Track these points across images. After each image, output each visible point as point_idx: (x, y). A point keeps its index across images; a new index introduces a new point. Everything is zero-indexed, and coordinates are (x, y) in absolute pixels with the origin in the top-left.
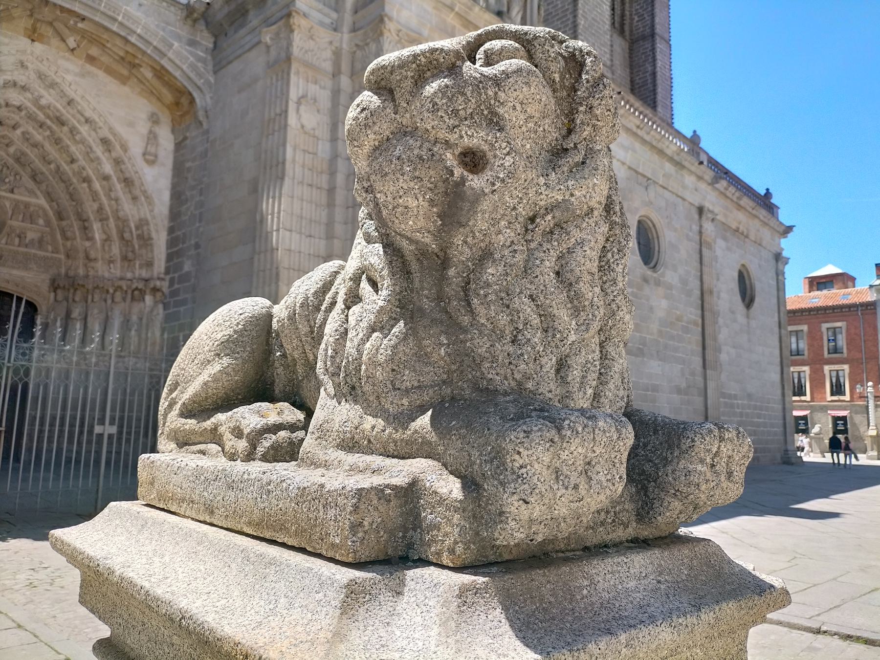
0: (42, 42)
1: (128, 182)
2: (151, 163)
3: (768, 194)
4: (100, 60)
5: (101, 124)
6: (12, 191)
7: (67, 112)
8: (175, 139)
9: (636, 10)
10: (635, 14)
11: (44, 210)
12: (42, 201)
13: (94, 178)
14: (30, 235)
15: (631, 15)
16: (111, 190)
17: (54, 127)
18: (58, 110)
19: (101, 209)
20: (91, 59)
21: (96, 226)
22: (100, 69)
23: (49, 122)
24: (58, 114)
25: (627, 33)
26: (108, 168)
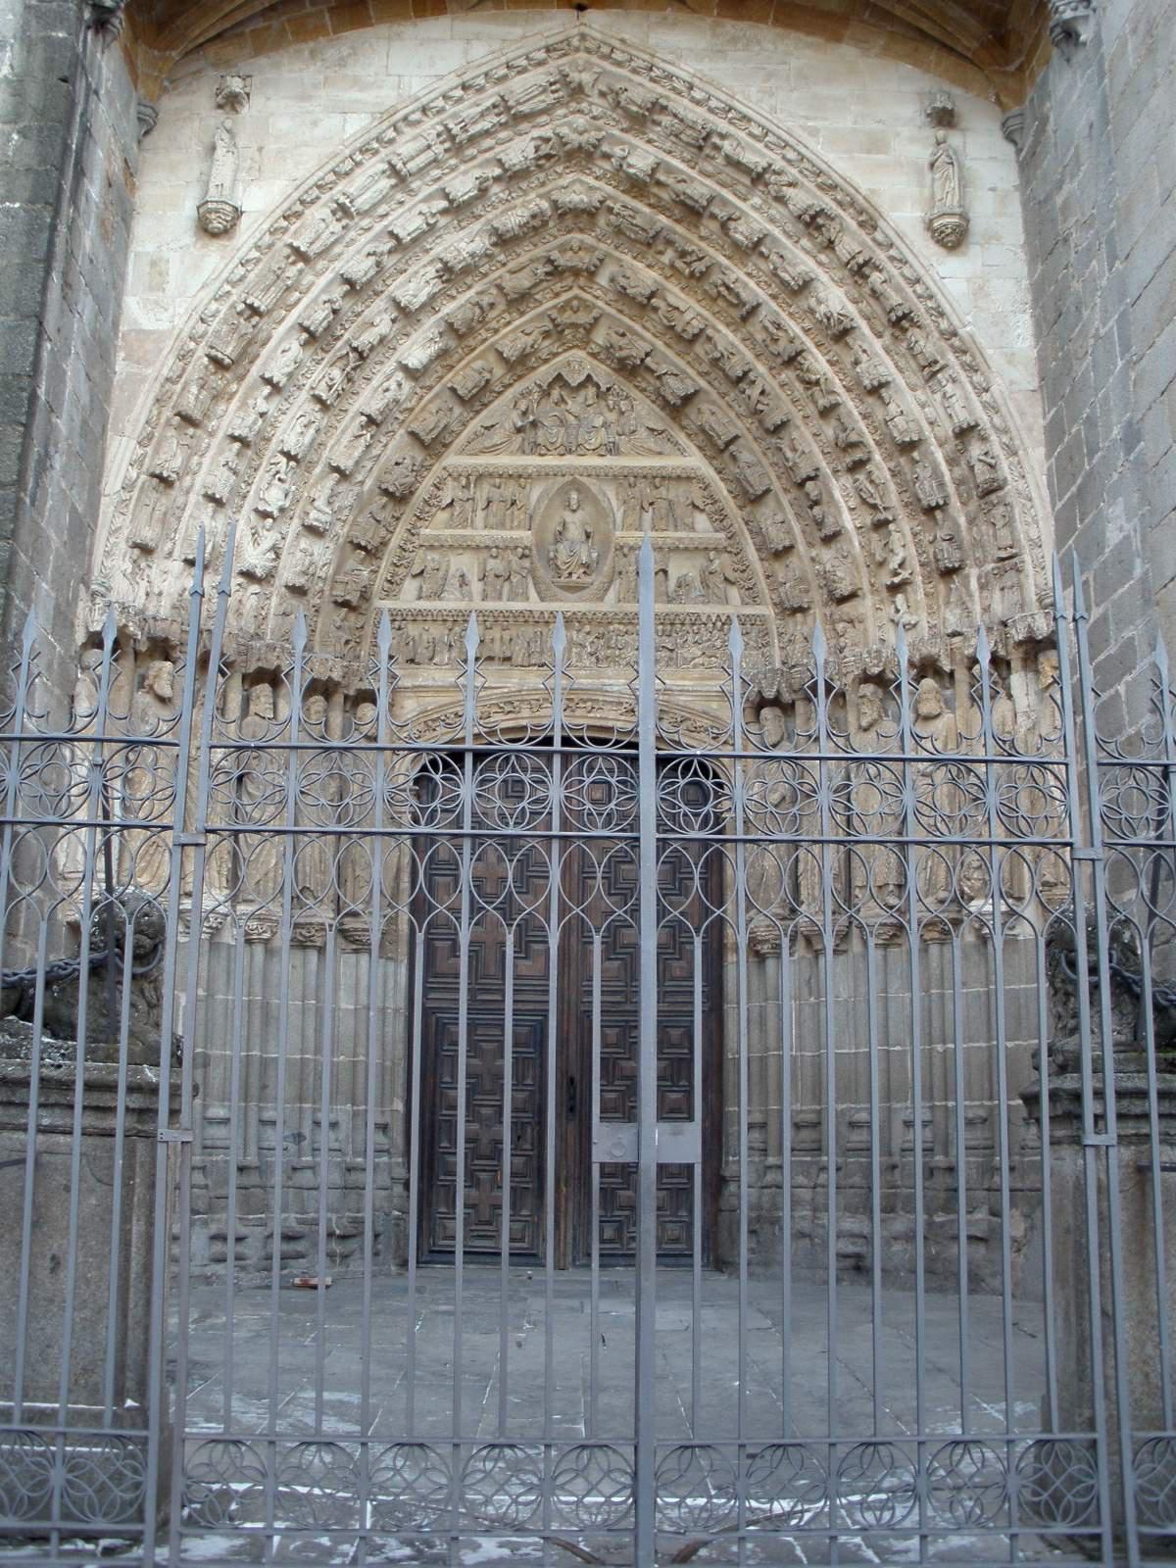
1: (900, 323)
2: (953, 237)
5: (793, 172)
6: (613, 449)
7: (701, 172)
12: (694, 460)
13: (809, 344)
17: (679, 228)
21: (840, 490)
23: (663, 220)
26: (834, 297)
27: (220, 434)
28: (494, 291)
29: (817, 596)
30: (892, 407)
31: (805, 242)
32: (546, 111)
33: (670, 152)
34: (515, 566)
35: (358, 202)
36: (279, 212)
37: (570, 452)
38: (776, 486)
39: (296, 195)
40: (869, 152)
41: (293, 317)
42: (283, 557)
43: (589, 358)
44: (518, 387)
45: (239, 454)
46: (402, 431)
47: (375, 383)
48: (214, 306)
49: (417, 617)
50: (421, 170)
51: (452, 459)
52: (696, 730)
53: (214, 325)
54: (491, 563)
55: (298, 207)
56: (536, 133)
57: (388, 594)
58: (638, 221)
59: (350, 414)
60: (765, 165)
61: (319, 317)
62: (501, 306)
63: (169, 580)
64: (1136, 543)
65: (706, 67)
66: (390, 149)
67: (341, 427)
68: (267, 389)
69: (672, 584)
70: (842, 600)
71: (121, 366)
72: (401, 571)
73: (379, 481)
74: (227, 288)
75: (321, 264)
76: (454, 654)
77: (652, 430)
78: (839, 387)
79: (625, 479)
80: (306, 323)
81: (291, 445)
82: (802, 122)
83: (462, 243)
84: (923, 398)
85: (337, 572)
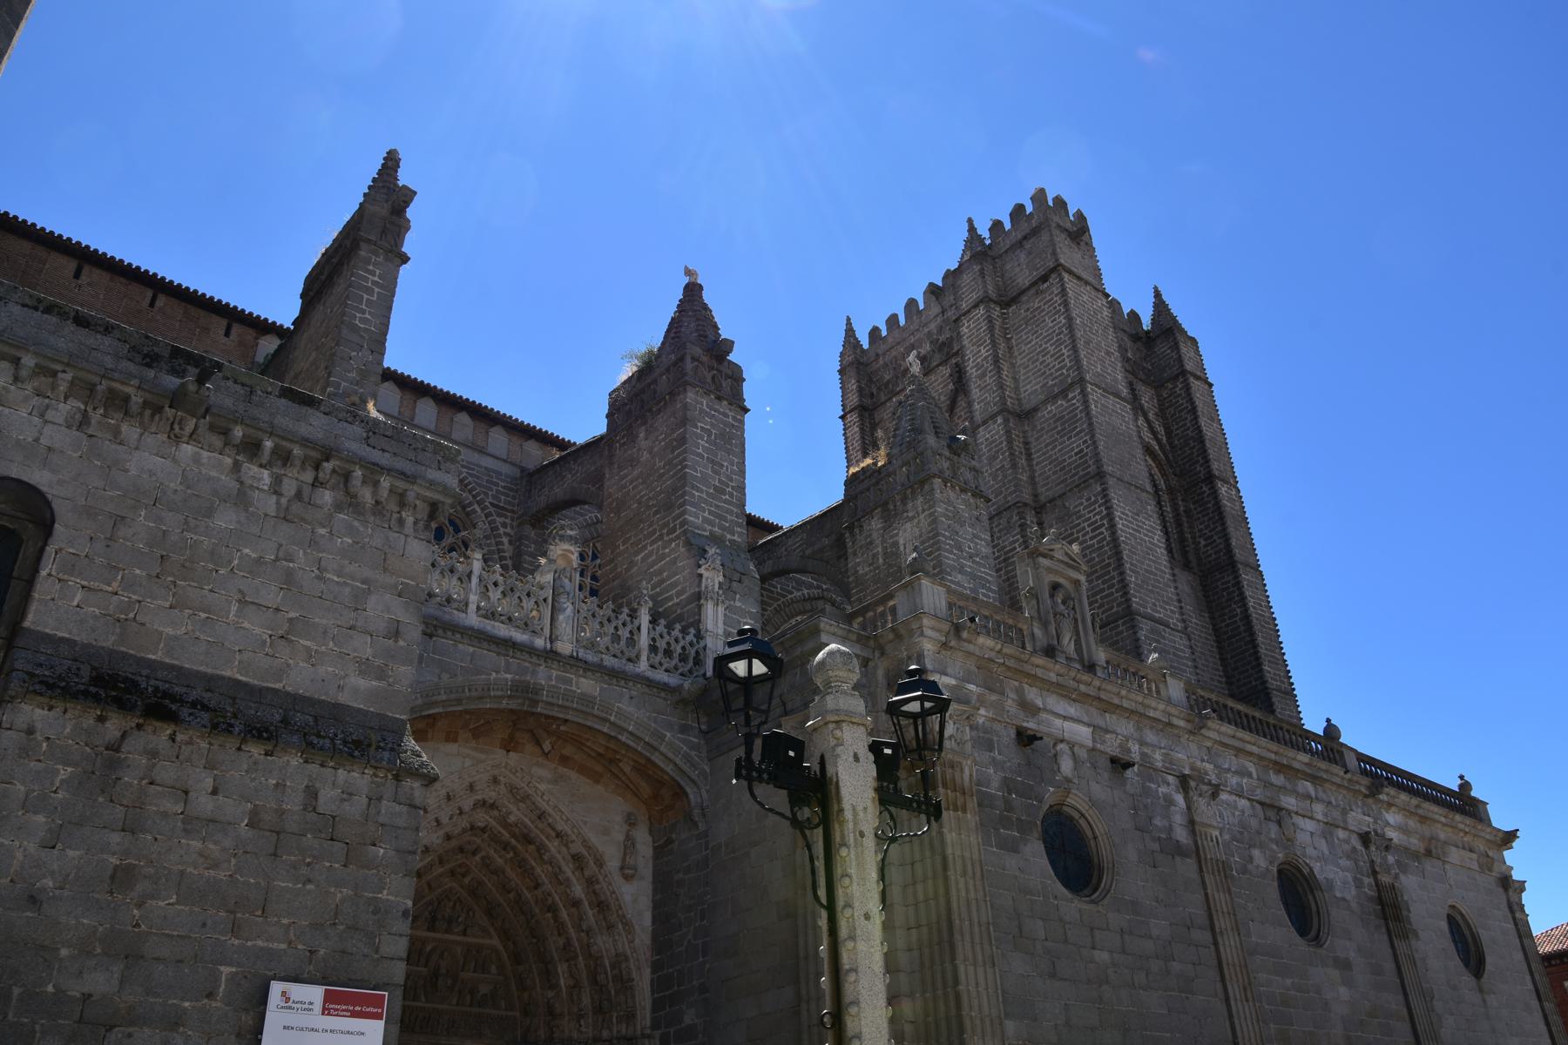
1: (601, 906)
2: (628, 878)
3: (1465, 786)
5: (574, 837)
6: (464, 933)
7: (536, 827)
8: (654, 842)
9: (1200, 531)
10: (1200, 537)
12: (495, 942)
15: (1194, 538)
16: (581, 919)
17: (519, 846)
19: (568, 944)
20: (564, 760)
21: (562, 968)
23: (513, 841)
24: (525, 831)
25: (1194, 563)
26: (578, 890)
65: (550, 787)
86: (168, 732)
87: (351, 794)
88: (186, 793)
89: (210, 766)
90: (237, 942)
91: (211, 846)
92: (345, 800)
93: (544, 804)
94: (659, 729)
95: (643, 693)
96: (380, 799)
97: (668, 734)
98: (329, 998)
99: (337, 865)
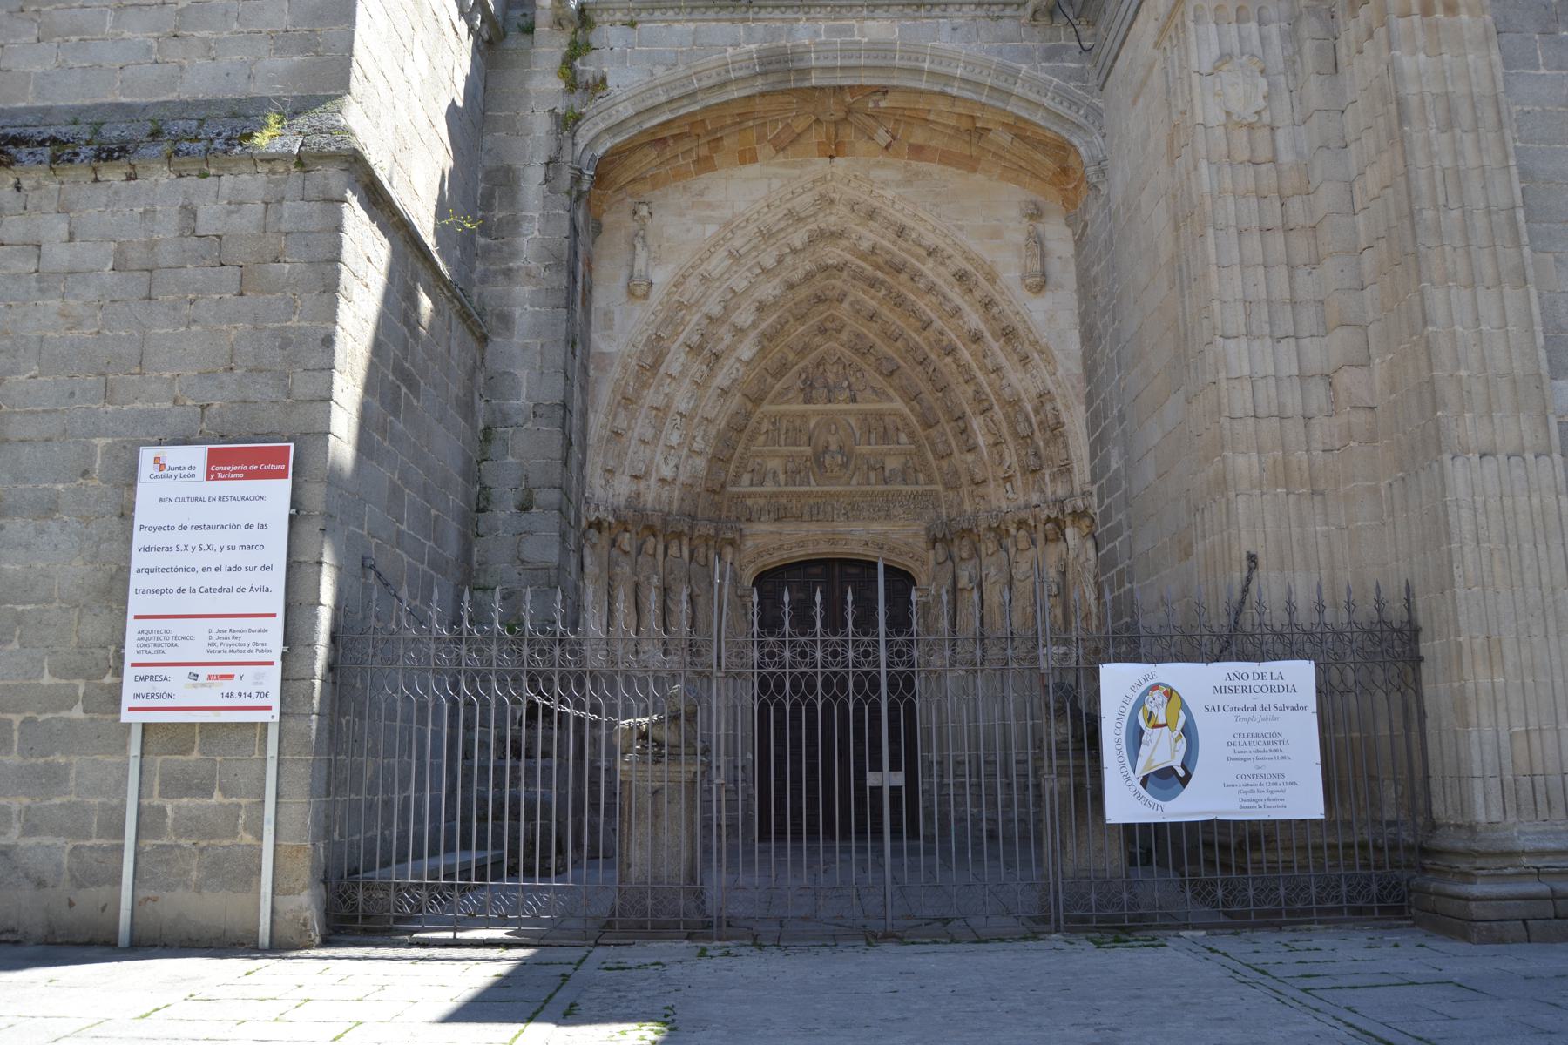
0: (844, 155)
1: (1008, 334)
2: (1040, 286)
4: (930, 147)
5: (950, 251)
6: (853, 400)
11: (903, 417)
12: (899, 404)
13: (960, 345)
14: (893, 463)
17: (888, 279)
18: (888, 252)
19: (978, 395)
20: (917, 151)
21: (977, 423)
22: (932, 161)
23: (879, 274)
24: (888, 257)
26: (974, 319)
27: (646, 406)
28: (787, 314)
29: (965, 479)
30: (1004, 381)
31: (957, 289)
32: (815, 214)
33: (882, 237)
34: (802, 467)
35: (713, 274)
36: (672, 283)
37: (830, 401)
38: (943, 420)
39: (680, 273)
40: (992, 239)
41: (681, 339)
42: (681, 468)
43: (839, 347)
44: (801, 365)
45: (656, 416)
46: (739, 395)
47: (724, 370)
48: (639, 338)
49: (750, 495)
50: (748, 252)
51: (766, 407)
52: (901, 554)
53: (640, 347)
54: (790, 465)
55: (682, 280)
56: (808, 227)
57: (734, 484)
58: (866, 273)
59: (712, 388)
60: (934, 247)
61: (696, 338)
62: (792, 321)
63: (622, 487)
64: (1123, 470)
65: (901, 190)
66: (730, 243)
67: (708, 395)
68: (669, 380)
69: (887, 473)
70: (977, 484)
71: (592, 373)
72: (741, 470)
73: (728, 424)
74: (646, 327)
75: (694, 309)
76: (772, 515)
77: (872, 387)
78: (974, 365)
79: (864, 416)
80: (689, 343)
81: (682, 408)
82: (955, 222)
83: (769, 290)
84: (1020, 377)
85: (707, 474)
86: (12, 181)
87: (241, 203)
88: (39, 246)
89: (64, 209)
90: (110, 408)
91: (72, 302)
92: (233, 212)
93: (899, 215)
94: (1008, 63)
95: (974, 18)
96: (280, 201)
97: (1024, 67)
98: (214, 458)
99: (228, 296)
